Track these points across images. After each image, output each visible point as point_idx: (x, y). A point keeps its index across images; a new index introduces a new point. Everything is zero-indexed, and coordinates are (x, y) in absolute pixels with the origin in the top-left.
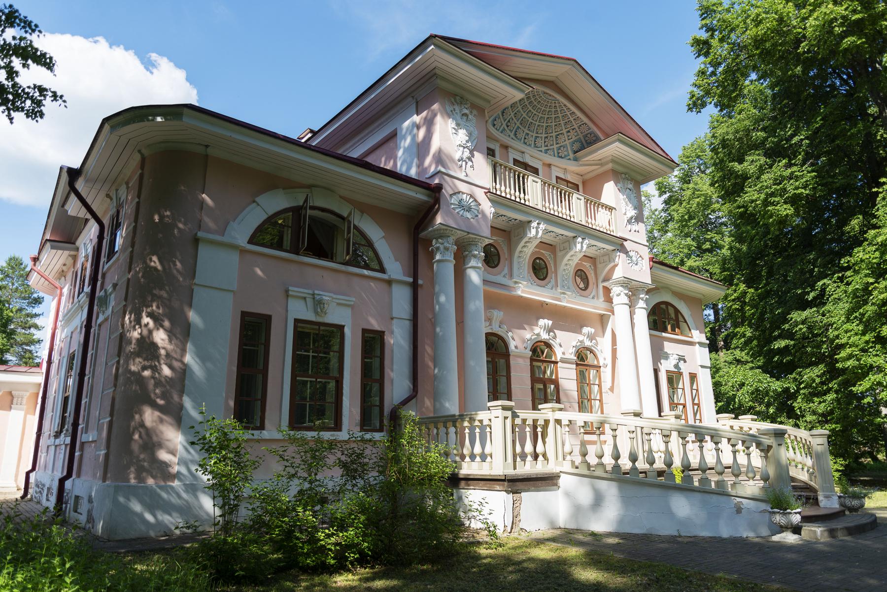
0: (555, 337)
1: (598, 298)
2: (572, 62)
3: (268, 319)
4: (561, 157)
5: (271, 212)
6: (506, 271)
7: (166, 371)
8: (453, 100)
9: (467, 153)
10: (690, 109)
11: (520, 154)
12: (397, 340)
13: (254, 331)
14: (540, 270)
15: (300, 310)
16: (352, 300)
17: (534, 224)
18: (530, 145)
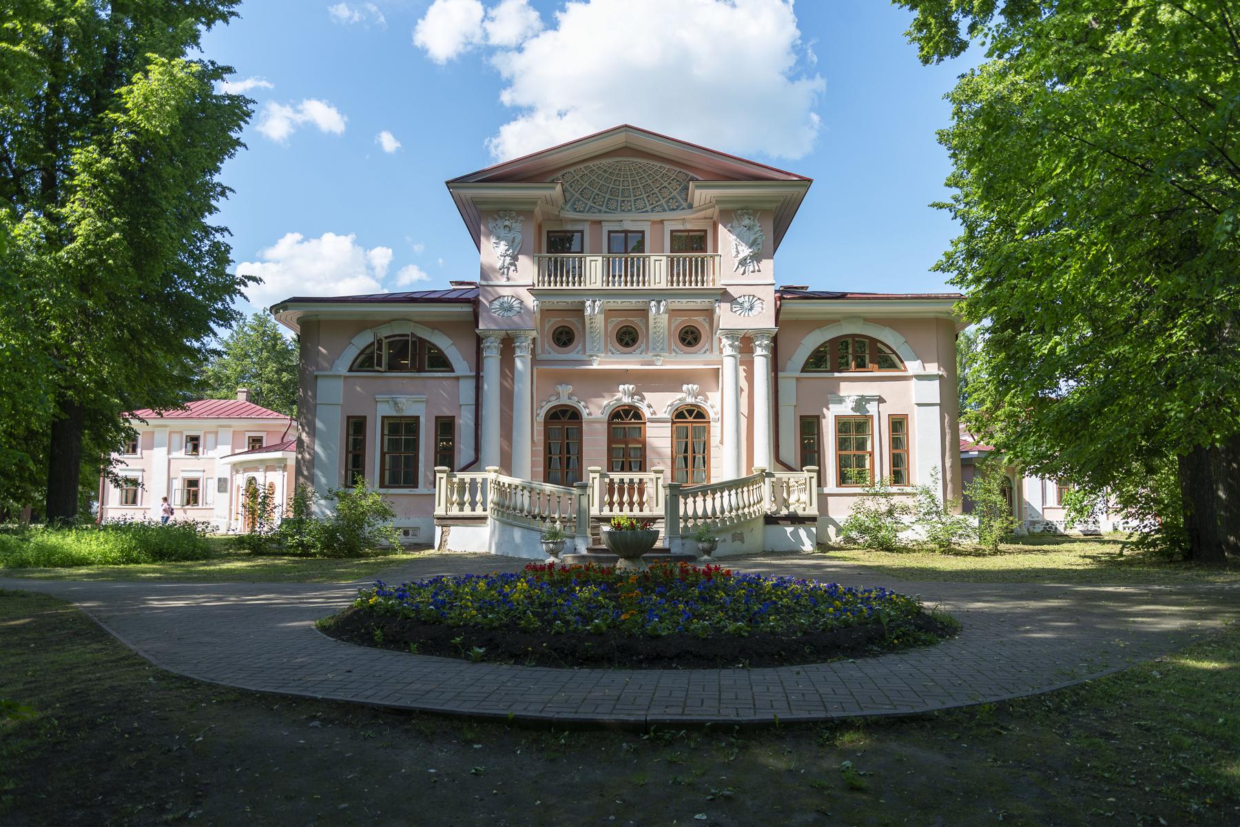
0: (643, 399)
3: (365, 417)
5: (362, 347)
6: (580, 347)
7: (307, 456)
9: (508, 260)
10: (926, 60)
12: (465, 422)
13: (357, 426)
14: (627, 338)
15: (385, 410)
16: (424, 397)
17: (588, 303)
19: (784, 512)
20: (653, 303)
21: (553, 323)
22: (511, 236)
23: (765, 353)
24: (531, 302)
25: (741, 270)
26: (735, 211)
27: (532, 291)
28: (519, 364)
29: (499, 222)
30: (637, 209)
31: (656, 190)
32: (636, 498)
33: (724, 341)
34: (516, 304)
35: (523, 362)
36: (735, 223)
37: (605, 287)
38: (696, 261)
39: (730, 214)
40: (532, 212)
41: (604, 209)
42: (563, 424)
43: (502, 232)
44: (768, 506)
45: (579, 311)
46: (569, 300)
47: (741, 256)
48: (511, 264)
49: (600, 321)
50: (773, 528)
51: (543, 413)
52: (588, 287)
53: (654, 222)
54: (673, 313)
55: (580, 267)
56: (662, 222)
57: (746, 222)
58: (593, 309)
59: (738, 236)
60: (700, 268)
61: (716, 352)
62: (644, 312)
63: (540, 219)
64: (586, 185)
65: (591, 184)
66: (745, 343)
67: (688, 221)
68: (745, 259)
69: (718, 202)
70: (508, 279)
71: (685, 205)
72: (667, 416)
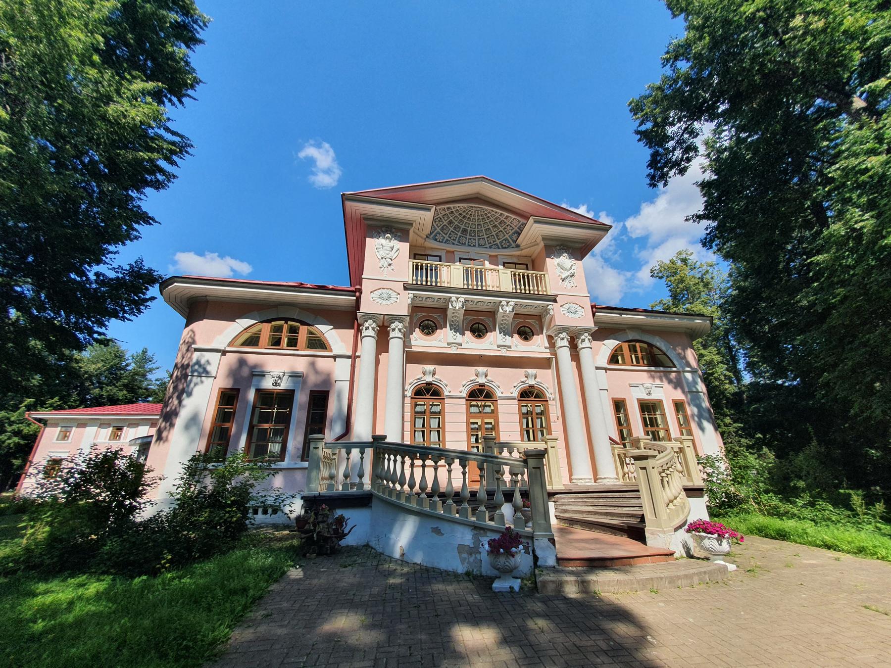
30: (480, 245)
40: (408, 231)
56: (496, 256)
64: (445, 223)
65: (450, 222)
69: (544, 239)
71: (513, 245)
72: (516, 394)
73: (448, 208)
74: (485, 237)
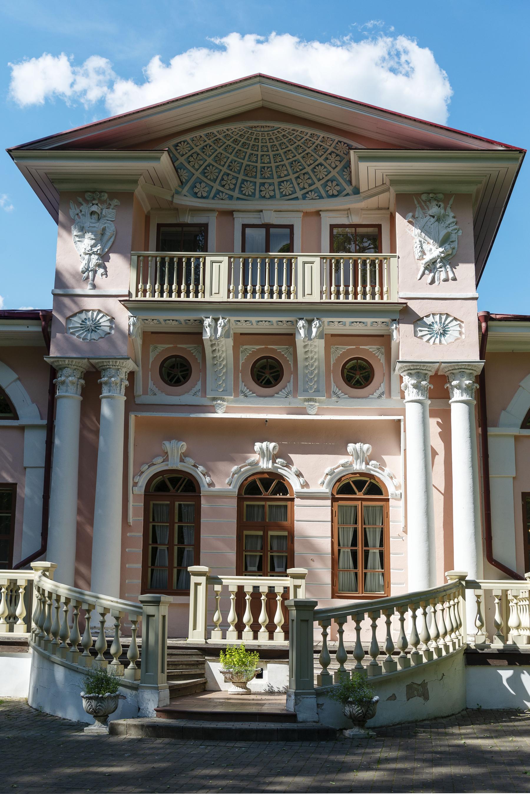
0: (289, 463)
1: (390, 395)
2: (258, 79)
4: (333, 196)
8: (80, 200)
9: (95, 259)
11: (256, 215)
14: (268, 373)
17: (207, 322)
18: (272, 197)
19: (497, 645)
20: (301, 323)
21: (161, 350)
22: (100, 226)
23: (465, 397)
24: (125, 319)
25: (429, 277)
26: (418, 195)
27: (128, 303)
28: (106, 410)
29: (85, 208)
31: (308, 169)
32: (263, 617)
33: (409, 381)
34: (104, 322)
35: (112, 407)
36: (419, 212)
37: (231, 299)
38: (364, 263)
39: (411, 199)
41: (236, 194)
42: (172, 502)
43: (88, 222)
44: (471, 635)
45: (195, 335)
46: (182, 317)
47: (428, 258)
48: (99, 266)
49: (226, 347)
50: (478, 672)
51: (143, 481)
52: (208, 298)
53: (307, 214)
54: (332, 339)
55: (197, 267)
56: (318, 213)
57: (434, 210)
58: (214, 330)
59: (423, 229)
60: (375, 273)
61: (396, 397)
62: (289, 338)
63: (147, 207)
64: (209, 160)
65: (218, 159)
66: (437, 384)
67: (356, 212)
68: (433, 262)
69: (393, 182)
70: (94, 287)
71: (349, 189)
72: (325, 489)
73: (207, 135)
74: (293, 177)
